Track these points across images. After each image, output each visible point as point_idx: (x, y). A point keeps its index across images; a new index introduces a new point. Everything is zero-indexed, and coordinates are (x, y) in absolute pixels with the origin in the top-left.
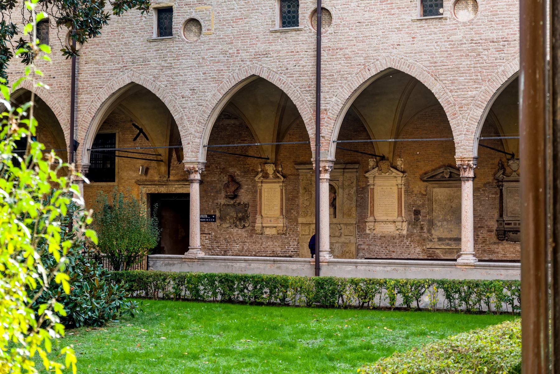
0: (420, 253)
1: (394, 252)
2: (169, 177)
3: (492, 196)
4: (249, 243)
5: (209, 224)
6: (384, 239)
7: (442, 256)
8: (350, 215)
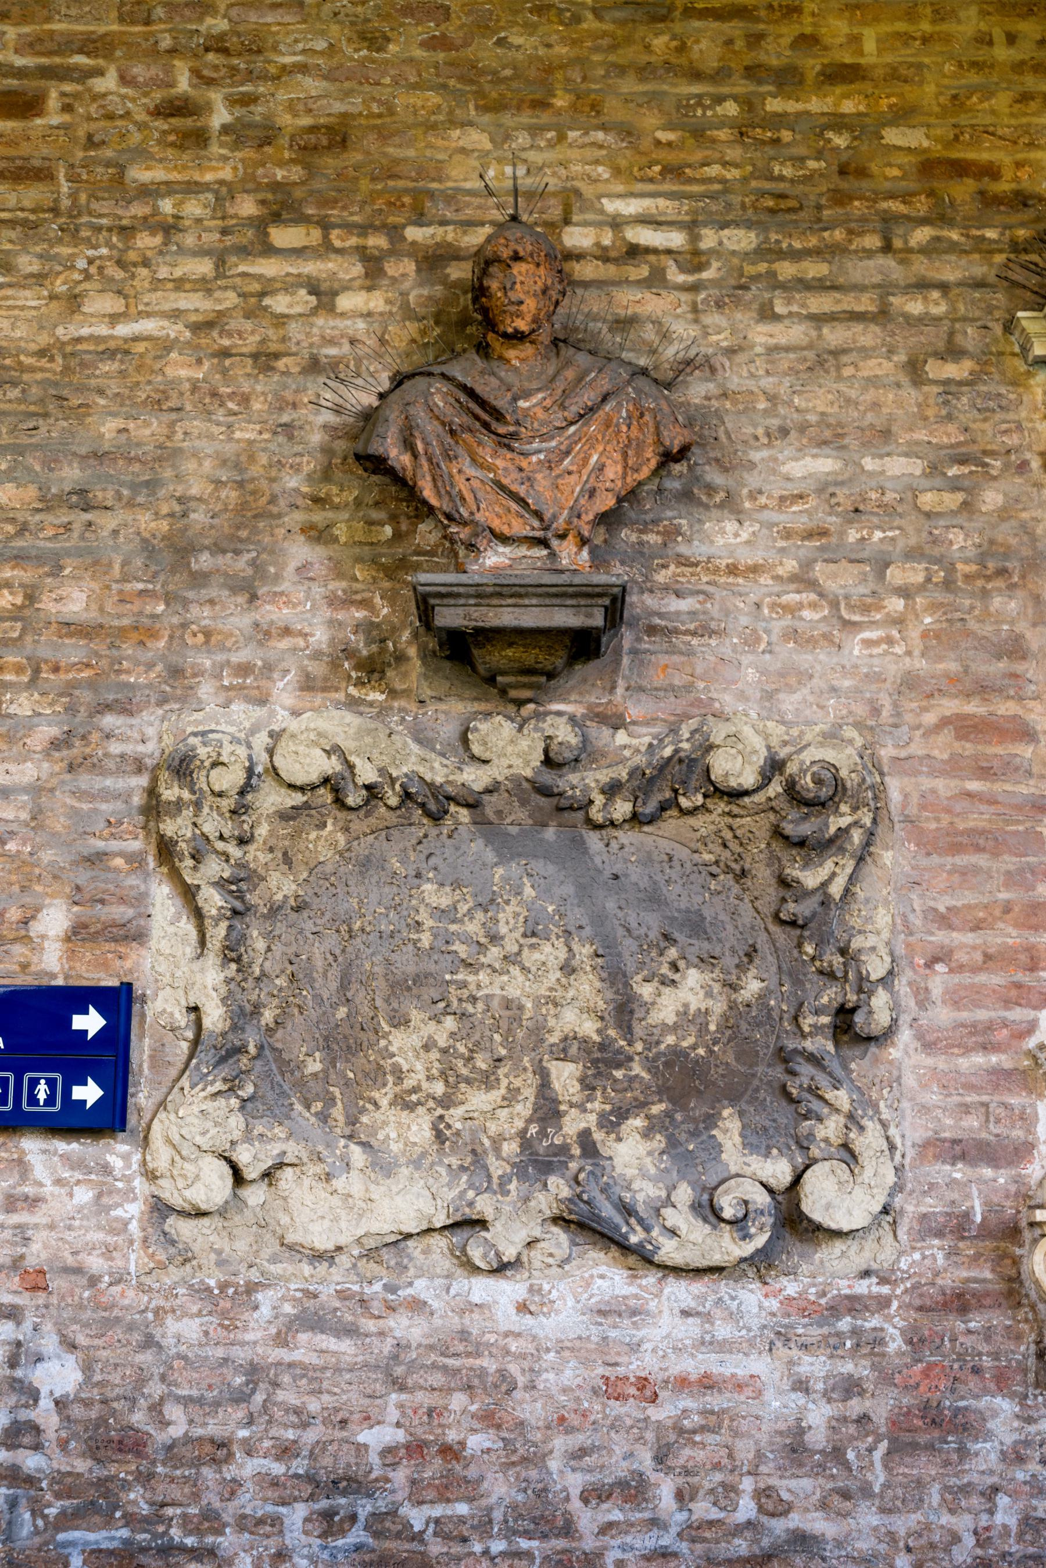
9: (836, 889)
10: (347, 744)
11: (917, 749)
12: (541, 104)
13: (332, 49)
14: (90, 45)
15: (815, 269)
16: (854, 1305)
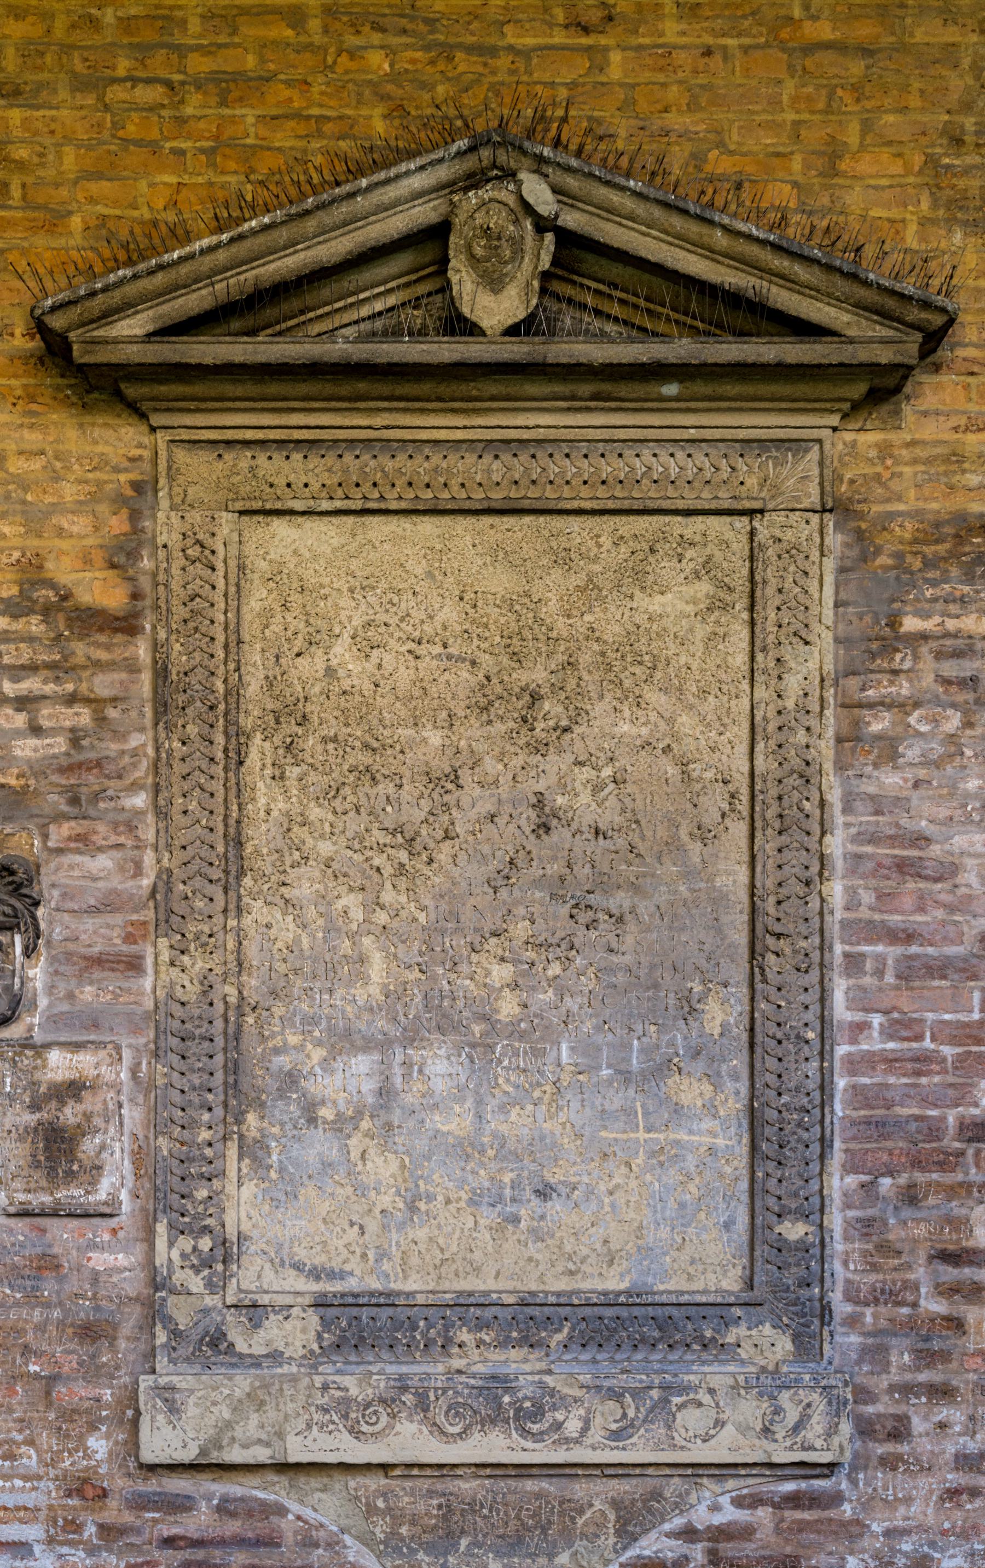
0: (33, 1532)
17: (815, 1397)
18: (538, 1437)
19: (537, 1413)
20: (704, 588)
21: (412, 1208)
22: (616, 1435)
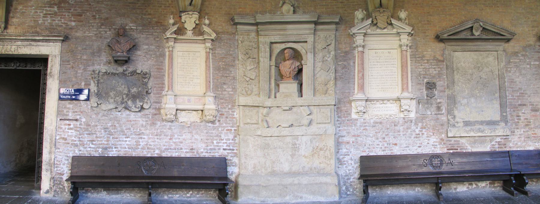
0: (437, 144)
1: (396, 144)
2: (6, 28)
3: (535, 63)
4: (148, 135)
5: (76, 105)
6: (380, 126)
7: (469, 147)
8: (326, 92)
9: (147, 81)
10: (107, 69)
11: (154, 70)
12: (124, 16)
13: (107, 11)
14: (87, 10)
15: (147, 31)
16: (147, 114)
17: (508, 129)
18: (484, 133)
19: (483, 131)
20: (493, 58)
21: (471, 113)
22: (490, 133)
